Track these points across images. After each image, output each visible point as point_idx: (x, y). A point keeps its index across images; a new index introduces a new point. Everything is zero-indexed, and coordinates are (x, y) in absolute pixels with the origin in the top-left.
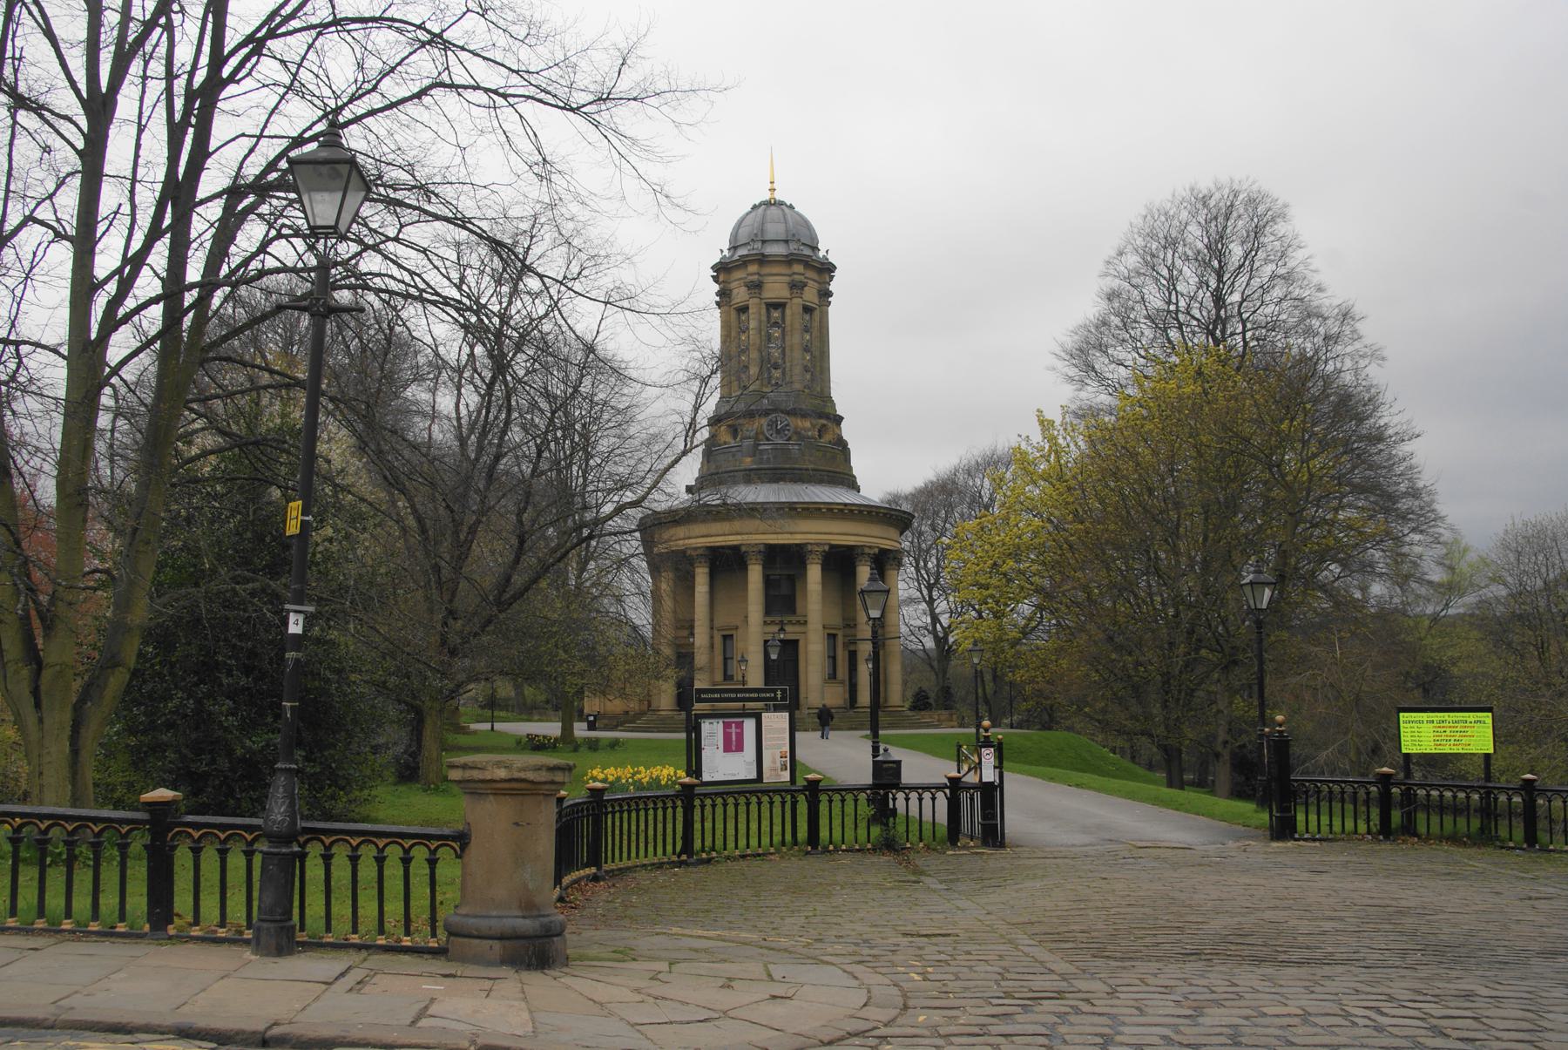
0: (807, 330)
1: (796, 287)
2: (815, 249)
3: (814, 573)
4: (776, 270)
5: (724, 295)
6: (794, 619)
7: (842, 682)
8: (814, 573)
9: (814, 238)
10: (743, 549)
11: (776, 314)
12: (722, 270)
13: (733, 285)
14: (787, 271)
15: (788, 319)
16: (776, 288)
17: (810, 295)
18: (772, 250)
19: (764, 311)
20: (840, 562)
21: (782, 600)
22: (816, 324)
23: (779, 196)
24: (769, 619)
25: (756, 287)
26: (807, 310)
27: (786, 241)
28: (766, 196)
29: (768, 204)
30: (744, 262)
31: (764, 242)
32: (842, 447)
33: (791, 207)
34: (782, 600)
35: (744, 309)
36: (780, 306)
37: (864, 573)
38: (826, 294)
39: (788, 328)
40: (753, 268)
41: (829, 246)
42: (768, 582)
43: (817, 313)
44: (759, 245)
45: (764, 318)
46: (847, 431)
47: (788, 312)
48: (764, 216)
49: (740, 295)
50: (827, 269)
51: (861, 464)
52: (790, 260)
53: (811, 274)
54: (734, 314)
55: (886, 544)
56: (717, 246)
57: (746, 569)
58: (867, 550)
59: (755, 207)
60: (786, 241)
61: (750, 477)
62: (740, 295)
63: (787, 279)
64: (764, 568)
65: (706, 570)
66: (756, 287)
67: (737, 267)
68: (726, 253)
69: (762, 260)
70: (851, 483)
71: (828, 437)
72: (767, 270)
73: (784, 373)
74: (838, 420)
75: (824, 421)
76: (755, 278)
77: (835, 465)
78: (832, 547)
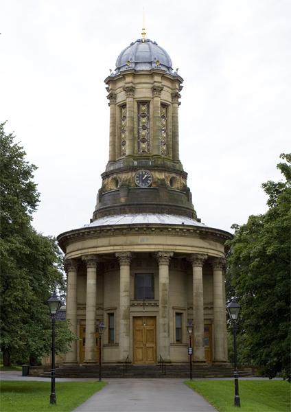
0: (163, 117)
1: (156, 90)
2: (169, 68)
3: (164, 271)
4: (143, 80)
5: (112, 97)
6: (152, 302)
7: (186, 345)
8: (164, 271)
9: (168, 60)
10: (117, 255)
11: (144, 108)
12: (110, 81)
13: (118, 91)
14: (152, 81)
15: (151, 110)
16: (143, 92)
17: (166, 96)
18: (139, 68)
19: (136, 106)
20: (181, 264)
21: (144, 290)
22: (170, 115)
23: (147, 37)
24: (136, 302)
25: (130, 90)
26: (164, 105)
27: (151, 63)
28: (140, 37)
29: (140, 41)
30: (122, 76)
31: (136, 63)
32: (186, 192)
33: (155, 43)
34: (144, 290)
35: (123, 106)
36: (145, 103)
37: (198, 272)
38: (176, 96)
39: (151, 117)
40: (129, 79)
41: (179, 66)
42: (135, 277)
43: (170, 109)
44: (133, 65)
45: (136, 110)
46: (190, 183)
47: (151, 106)
48: (137, 49)
49: (121, 97)
50: (177, 80)
51: (197, 203)
52: (152, 74)
53: (165, 83)
54: (118, 109)
55: (213, 253)
56: (110, 68)
57: (119, 266)
58: (199, 257)
59: (132, 44)
60: (151, 63)
61: (122, 210)
62: (121, 97)
63: (150, 86)
64: (131, 269)
65: (94, 270)
66: (130, 90)
67: (120, 79)
68: (115, 72)
69: (135, 74)
70: (191, 214)
71: (177, 185)
72: (137, 80)
73: (148, 145)
74: (184, 175)
75: (174, 175)
76: (130, 85)
77: (180, 202)
78: (176, 254)
